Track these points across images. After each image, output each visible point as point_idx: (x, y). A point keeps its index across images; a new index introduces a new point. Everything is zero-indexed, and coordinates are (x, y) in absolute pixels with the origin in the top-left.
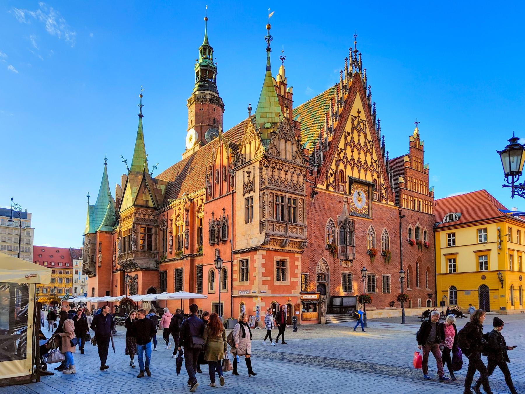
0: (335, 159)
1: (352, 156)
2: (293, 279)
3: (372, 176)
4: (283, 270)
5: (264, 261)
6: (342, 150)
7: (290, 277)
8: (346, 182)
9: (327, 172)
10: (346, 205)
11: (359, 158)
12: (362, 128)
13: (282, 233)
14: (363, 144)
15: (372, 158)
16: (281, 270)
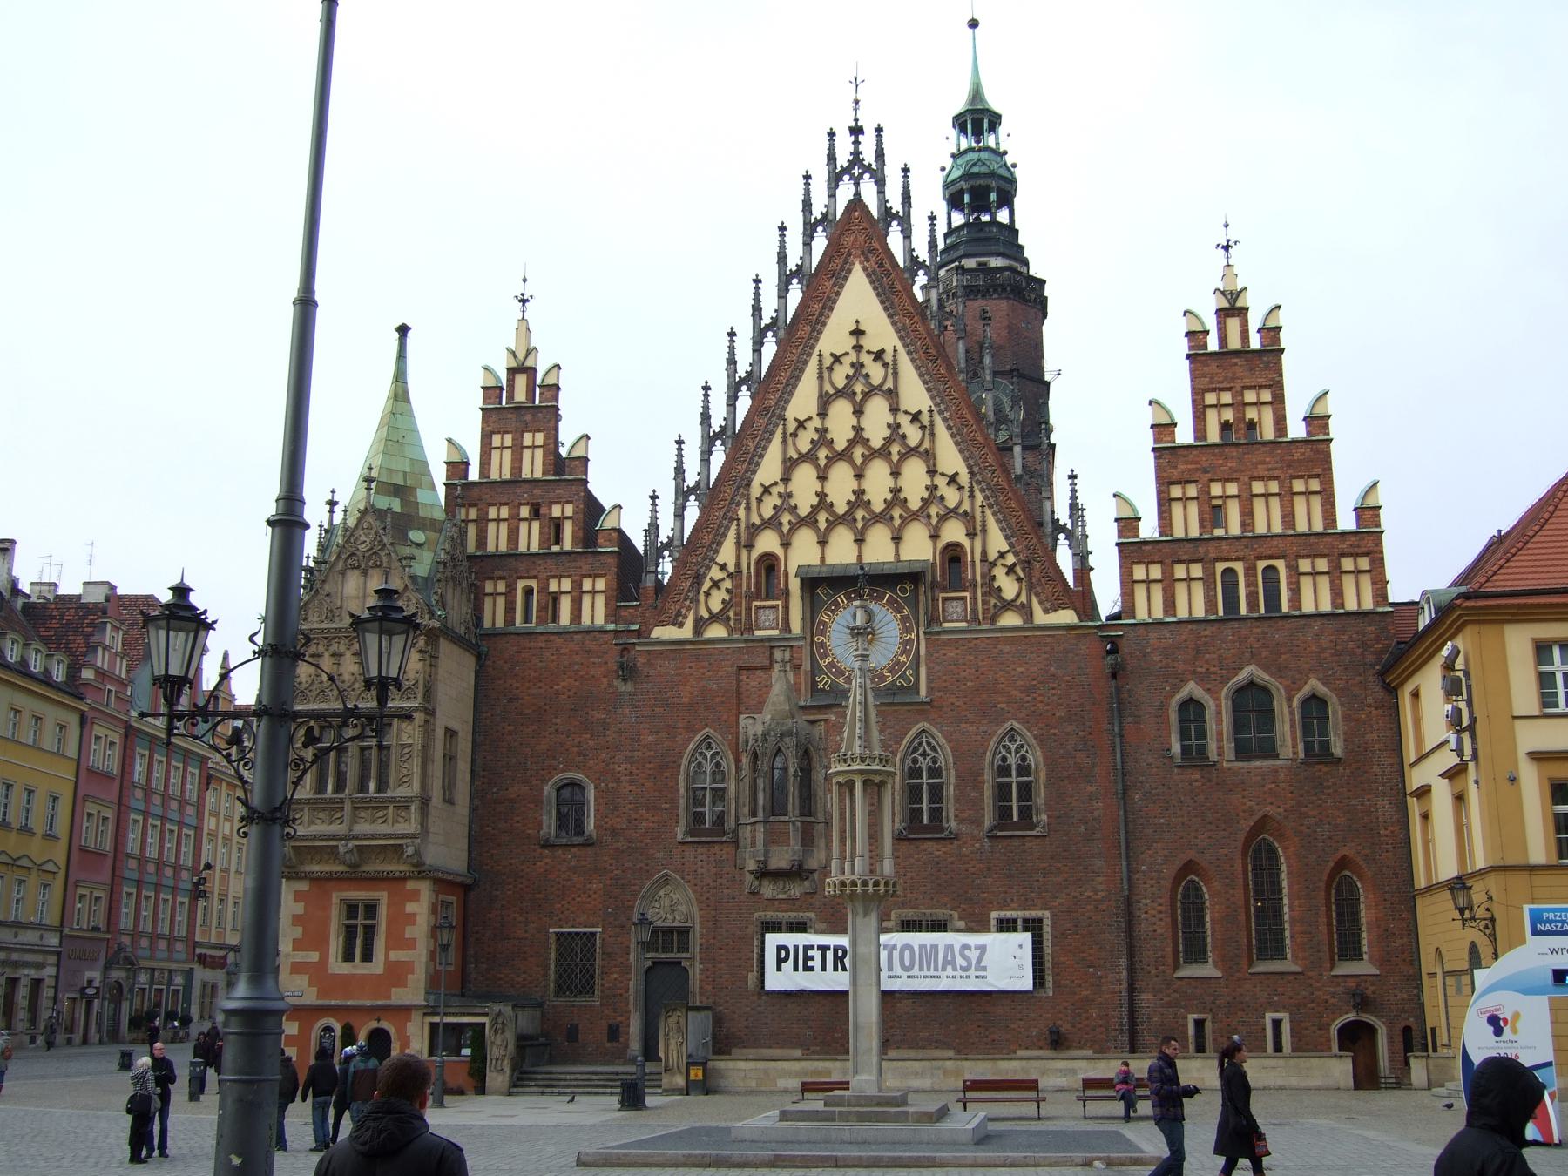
0: (734, 527)
1: (822, 495)
2: (394, 956)
3: (934, 537)
4: (370, 931)
5: (299, 908)
6: (766, 490)
7: (388, 949)
8: (786, 594)
9: (698, 579)
10: (791, 676)
11: (859, 493)
12: (876, 381)
13: (335, 828)
14: (876, 433)
15: (932, 472)
16: (360, 931)
